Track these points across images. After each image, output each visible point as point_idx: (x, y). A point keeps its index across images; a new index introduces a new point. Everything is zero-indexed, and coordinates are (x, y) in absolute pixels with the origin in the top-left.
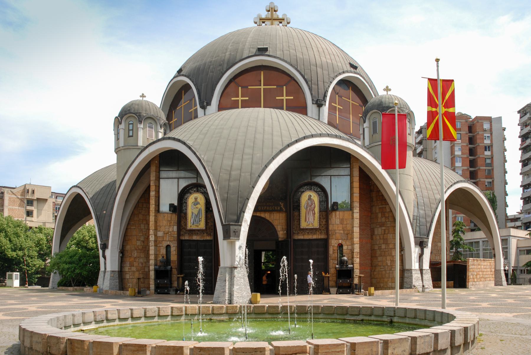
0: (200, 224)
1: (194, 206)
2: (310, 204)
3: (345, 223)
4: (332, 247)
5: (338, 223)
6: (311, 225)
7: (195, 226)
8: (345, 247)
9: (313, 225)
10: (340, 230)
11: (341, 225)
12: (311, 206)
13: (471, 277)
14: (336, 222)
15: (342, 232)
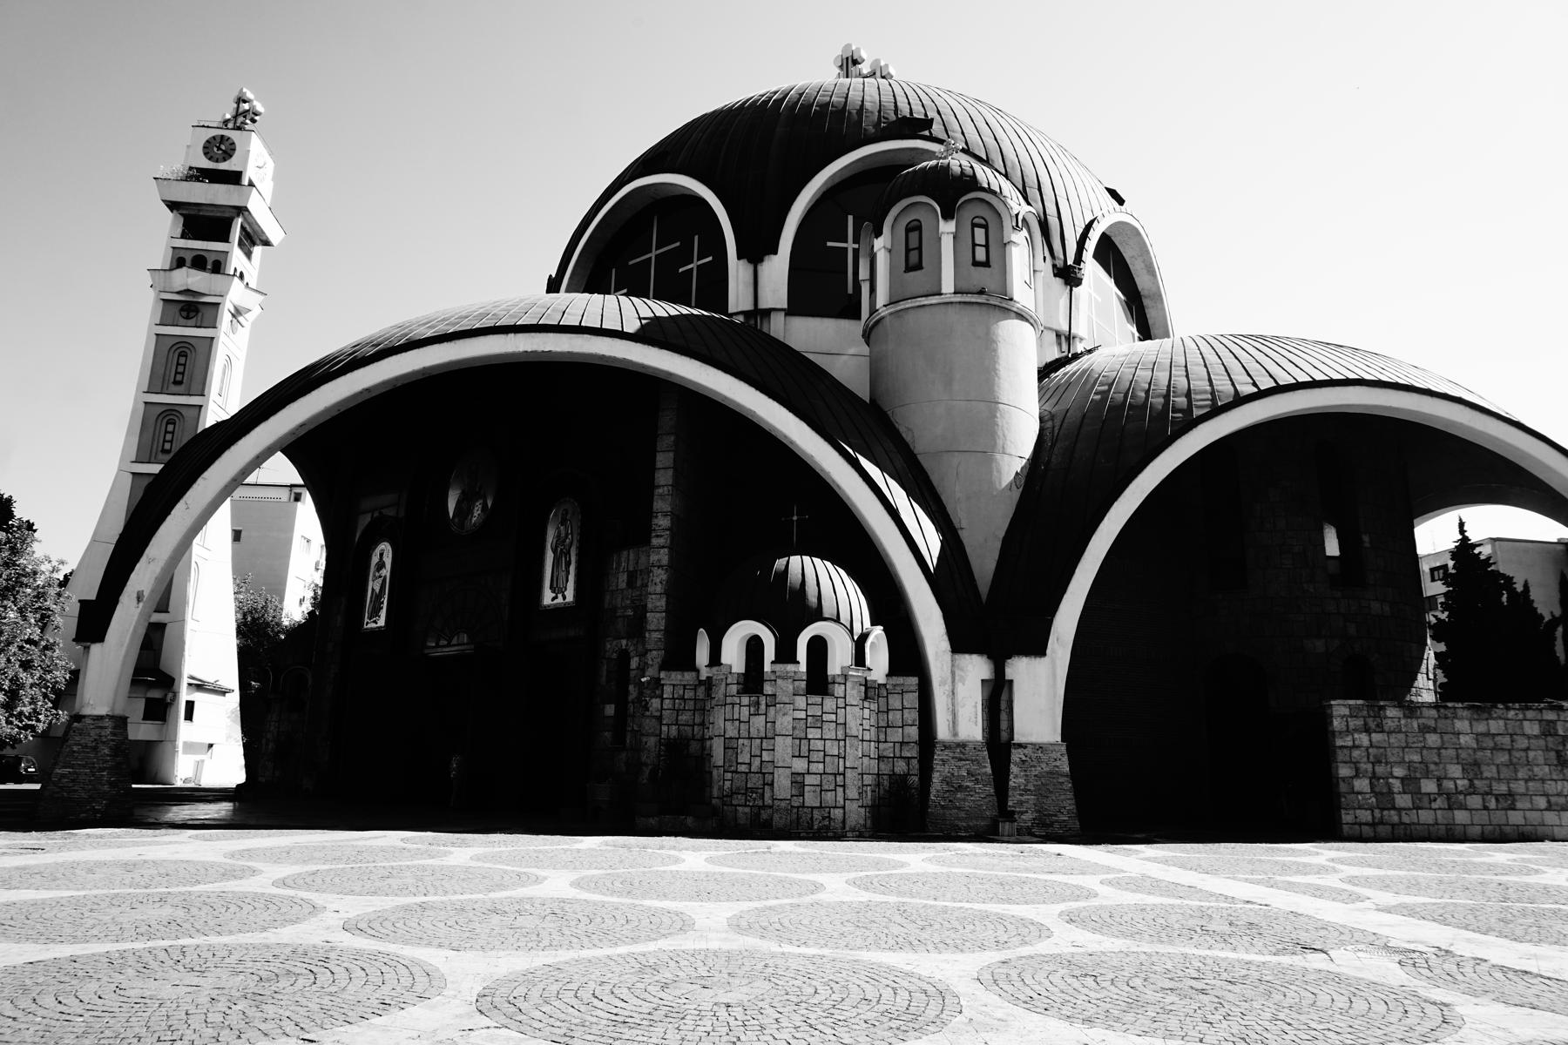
0: (379, 617)
1: (377, 574)
2: (563, 535)
3: (638, 585)
4: (605, 662)
5: (623, 585)
6: (560, 596)
7: (375, 622)
8: (634, 663)
9: (564, 598)
10: (625, 608)
11: (630, 590)
12: (564, 541)
13: (1362, 784)
14: (620, 580)
15: (630, 612)
